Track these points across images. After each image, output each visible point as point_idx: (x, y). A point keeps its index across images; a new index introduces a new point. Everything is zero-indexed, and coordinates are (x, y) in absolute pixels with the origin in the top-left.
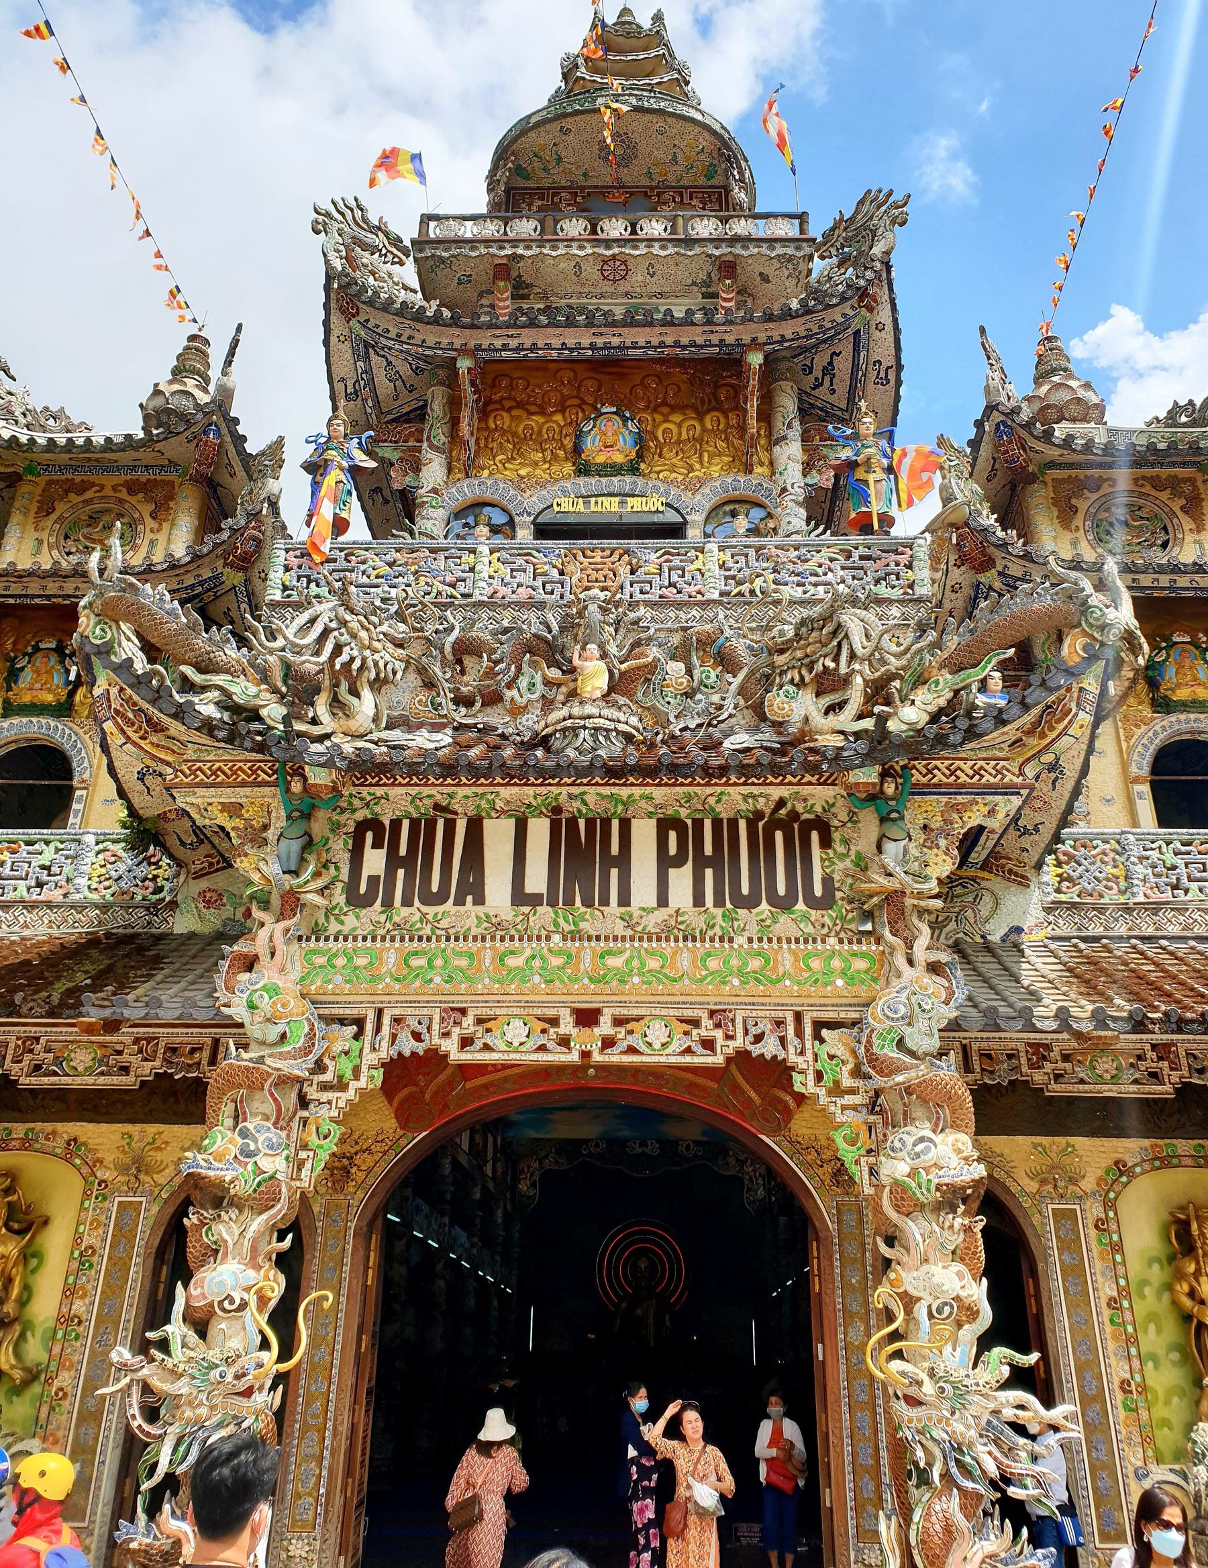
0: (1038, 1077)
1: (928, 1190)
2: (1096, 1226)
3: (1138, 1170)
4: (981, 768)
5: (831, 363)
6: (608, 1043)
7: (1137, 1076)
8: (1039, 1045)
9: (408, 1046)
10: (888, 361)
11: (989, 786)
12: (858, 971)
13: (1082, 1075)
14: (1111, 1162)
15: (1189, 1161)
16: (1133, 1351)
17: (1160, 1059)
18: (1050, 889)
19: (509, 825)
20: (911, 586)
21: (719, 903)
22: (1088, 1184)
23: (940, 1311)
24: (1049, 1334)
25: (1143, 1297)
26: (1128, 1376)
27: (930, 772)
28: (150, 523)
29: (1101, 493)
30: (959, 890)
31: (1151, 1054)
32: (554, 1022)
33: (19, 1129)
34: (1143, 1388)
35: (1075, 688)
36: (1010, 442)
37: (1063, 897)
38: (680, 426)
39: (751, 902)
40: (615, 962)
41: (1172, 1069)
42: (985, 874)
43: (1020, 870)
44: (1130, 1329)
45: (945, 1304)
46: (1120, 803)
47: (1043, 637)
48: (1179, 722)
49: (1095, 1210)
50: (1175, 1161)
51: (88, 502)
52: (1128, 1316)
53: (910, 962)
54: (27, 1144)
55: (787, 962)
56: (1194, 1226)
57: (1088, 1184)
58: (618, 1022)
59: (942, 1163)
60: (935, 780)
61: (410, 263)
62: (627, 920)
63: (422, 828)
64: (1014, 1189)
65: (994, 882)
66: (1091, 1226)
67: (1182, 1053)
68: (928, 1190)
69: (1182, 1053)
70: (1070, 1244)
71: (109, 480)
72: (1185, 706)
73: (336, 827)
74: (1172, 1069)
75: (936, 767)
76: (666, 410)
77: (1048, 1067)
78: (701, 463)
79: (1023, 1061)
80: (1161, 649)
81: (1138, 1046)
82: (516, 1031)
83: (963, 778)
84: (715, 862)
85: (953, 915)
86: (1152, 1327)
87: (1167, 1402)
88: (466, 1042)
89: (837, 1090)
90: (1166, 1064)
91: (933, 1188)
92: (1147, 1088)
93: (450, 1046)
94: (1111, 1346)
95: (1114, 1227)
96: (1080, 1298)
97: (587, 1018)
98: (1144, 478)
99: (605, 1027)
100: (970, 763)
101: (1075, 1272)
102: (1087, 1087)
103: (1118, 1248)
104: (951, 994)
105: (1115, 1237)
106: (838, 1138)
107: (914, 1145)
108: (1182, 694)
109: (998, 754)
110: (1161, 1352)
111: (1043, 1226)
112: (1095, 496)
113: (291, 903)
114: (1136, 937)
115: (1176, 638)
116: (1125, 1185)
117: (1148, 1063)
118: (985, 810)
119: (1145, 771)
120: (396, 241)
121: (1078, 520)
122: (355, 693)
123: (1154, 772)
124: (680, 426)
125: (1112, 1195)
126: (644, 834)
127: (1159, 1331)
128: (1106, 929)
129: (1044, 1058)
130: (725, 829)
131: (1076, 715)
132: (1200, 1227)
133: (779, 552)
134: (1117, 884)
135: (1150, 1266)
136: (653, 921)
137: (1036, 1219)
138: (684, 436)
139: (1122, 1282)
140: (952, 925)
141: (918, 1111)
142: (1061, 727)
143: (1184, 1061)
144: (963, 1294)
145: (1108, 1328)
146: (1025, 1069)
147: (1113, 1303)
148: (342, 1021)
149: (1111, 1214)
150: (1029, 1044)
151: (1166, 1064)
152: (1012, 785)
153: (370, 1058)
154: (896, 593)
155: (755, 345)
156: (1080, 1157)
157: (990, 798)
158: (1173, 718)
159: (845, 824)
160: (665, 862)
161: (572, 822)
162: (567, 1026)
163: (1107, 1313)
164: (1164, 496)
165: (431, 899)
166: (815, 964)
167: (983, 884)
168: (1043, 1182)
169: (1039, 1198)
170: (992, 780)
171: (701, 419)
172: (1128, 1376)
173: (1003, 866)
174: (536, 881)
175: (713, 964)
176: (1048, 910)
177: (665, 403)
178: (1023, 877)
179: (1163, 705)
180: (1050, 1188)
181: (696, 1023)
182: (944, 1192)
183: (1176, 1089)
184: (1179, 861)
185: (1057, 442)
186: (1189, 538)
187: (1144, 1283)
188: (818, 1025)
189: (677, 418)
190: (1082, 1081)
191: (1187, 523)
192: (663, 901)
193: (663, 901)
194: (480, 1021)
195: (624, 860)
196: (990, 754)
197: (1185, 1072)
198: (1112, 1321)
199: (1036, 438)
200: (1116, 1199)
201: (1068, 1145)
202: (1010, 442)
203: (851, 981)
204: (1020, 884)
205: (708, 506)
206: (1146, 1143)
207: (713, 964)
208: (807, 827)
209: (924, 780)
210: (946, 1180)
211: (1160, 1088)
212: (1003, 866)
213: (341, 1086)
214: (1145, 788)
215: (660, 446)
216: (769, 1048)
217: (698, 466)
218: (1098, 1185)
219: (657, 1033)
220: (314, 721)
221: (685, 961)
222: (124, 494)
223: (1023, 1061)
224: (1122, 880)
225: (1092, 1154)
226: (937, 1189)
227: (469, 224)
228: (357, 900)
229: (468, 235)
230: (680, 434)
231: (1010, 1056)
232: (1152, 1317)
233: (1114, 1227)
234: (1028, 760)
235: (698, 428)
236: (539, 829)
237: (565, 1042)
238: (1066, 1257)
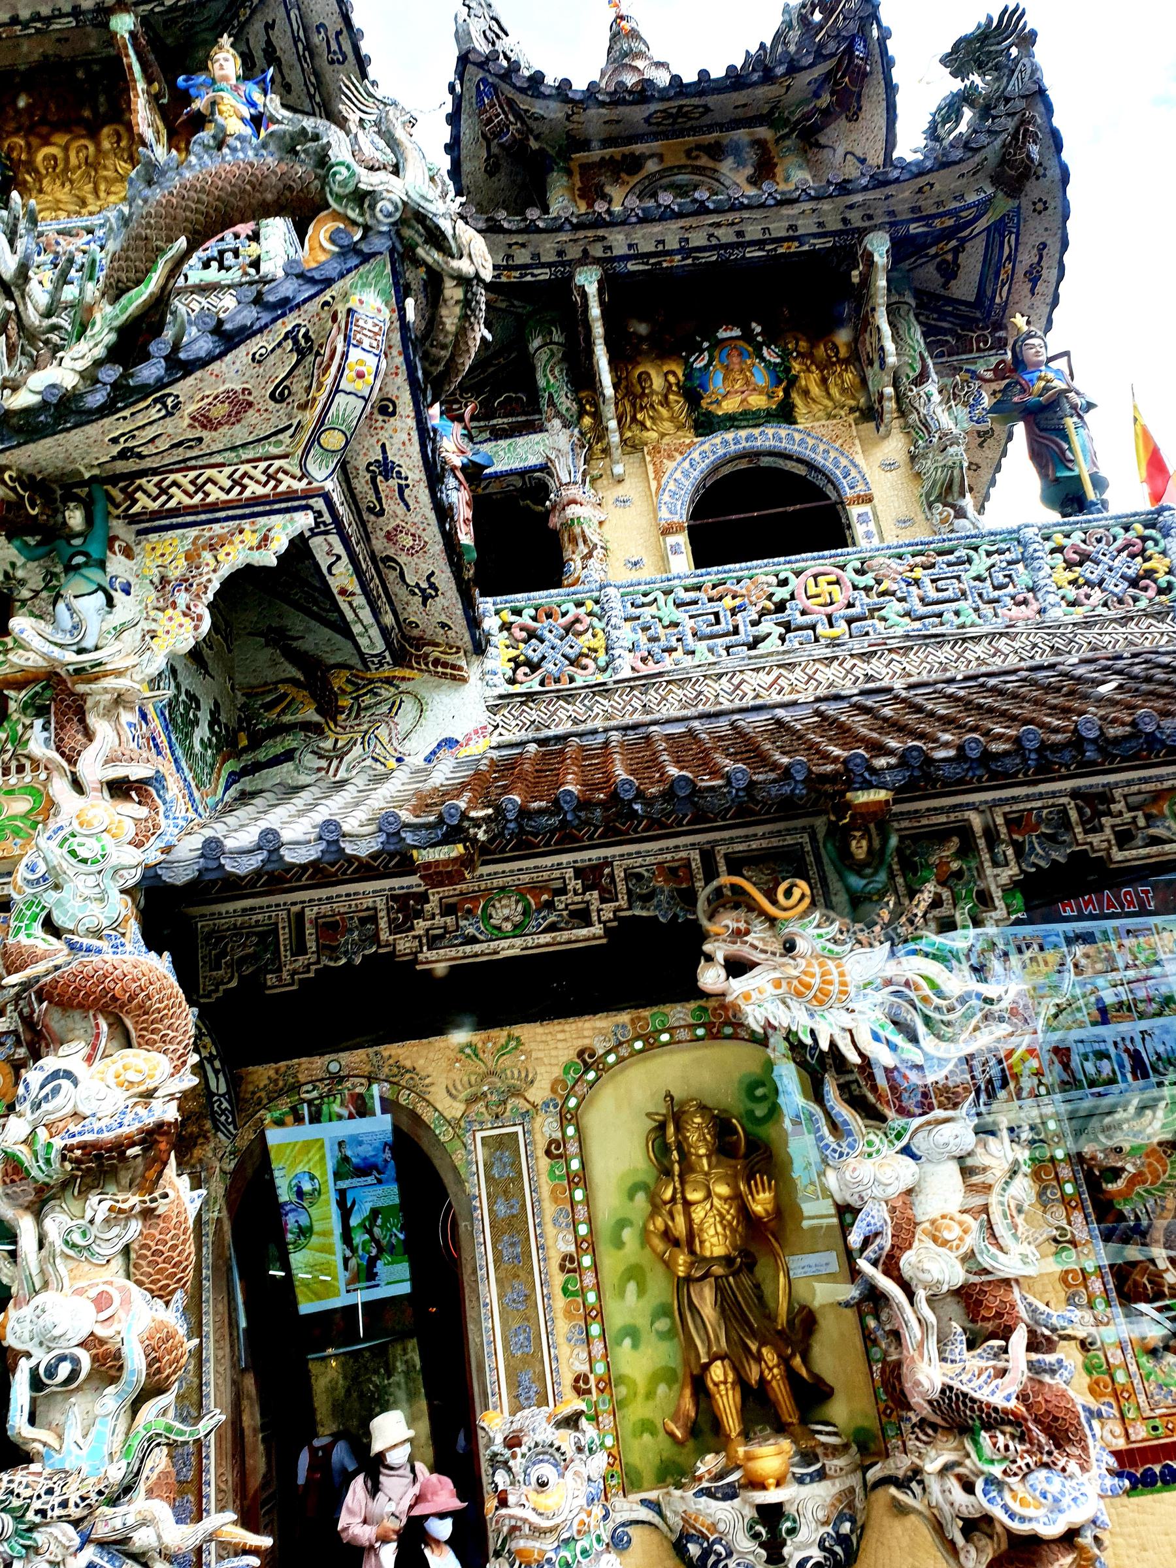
0: (404, 945)
1: (48, 1161)
2: (548, 1153)
3: (611, 1058)
4: (245, 474)
5: (269, 42)
7: (553, 918)
8: (408, 896)
10: (334, 23)
11: (256, 501)
12: (14, 817)
13: (471, 931)
14: (572, 1054)
15: (683, 1034)
16: (595, 1329)
17: (586, 889)
18: (499, 680)
23: (51, 1372)
24: (471, 1327)
25: (619, 1244)
26: (585, 1368)
27: (163, 491)
29: (643, 173)
30: (368, 700)
31: (575, 884)
34: (608, 1383)
35: (341, 316)
36: (492, 106)
37: (517, 689)
38: (66, 149)
41: (603, 900)
42: (407, 673)
43: (450, 659)
44: (591, 1297)
45: (62, 1358)
47: (545, 357)
48: (725, 443)
49: (546, 1127)
50: (665, 1037)
52: (589, 1279)
53: (77, 785)
56: (671, 1129)
57: (539, 1093)
59: (85, 1110)
60: (172, 504)
64: (428, 1116)
65: (418, 681)
66: (540, 1153)
67: (620, 874)
68: (48, 1161)
69: (620, 874)
70: (506, 1186)
72: (732, 421)
74: (603, 900)
75: (174, 483)
76: (44, 130)
77: (421, 925)
78: (96, 191)
79: (383, 924)
80: (702, 352)
81: (556, 874)
83: (215, 494)
85: (359, 736)
86: (632, 1287)
87: (650, 1395)
90: (596, 894)
91: (54, 1155)
92: (565, 936)
94: (562, 1326)
95: (573, 1148)
98: (699, 147)
100: (228, 470)
101: (511, 1228)
102: (477, 948)
103: (582, 1179)
105: (575, 1165)
107: (42, 1087)
108: (730, 406)
109: (275, 451)
110: (642, 1322)
111: (470, 1163)
112: (637, 178)
114: (616, 729)
115: (722, 334)
116: (592, 1084)
117: (570, 898)
118: (254, 540)
123: (695, 515)
124: (66, 149)
125: (572, 1102)
127: (641, 1291)
128: (576, 722)
129: (419, 914)
131: (345, 355)
132: (678, 1129)
133: (61, 239)
134: (595, 660)
135: (631, 1197)
137: (458, 1157)
138: (73, 161)
139: (583, 1230)
140: (357, 750)
142: (328, 380)
143: (621, 887)
144: (101, 1332)
145: (560, 1302)
146: (384, 936)
149: (571, 1131)
150: (394, 898)
151: (596, 894)
152: (290, 495)
156: (528, 1054)
157: (262, 521)
158: (717, 439)
159: (37, 593)
163: (558, 1279)
167: (403, 686)
168: (472, 1100)
170: (260, 491)
171: (94, 135)
172: (585, 1368)
173: (426, 656)
176: (493, 709)
177: (44, 121)
178: (454, 667)
179: (705, 425)
180: (480, 1106)
182: (77, 1161)
183: (607, 930)
184: (680, 615)
185: (547, 92)
187: (622, 1223)
189: (61, 139)
190: (473, 940)
196: (260, 451)
197: (623, 903)
198: (565, 1291)
199: (522, 90)
200: (578, 1106)
201: (510, 1037)
202: (492, 106)
204: (454, 678)
206: (624, 1017)
209: (155, 506)
210: (89, 1137)
211: (584, 932)
212: (426, 656)
214: (682, 539)
215: (39, 179)
217: (90, 198)
218: (553, 1090)
223: (383, 924)
224: (602, 652)
225: (548, 1048)
226: (64, 1158)
230: (67, 159)
231: (363, 921)
232: (634, 1273)
233: (573, 1148)
234: (307, 451)
235: (92, 149)
238: (501, 1209)
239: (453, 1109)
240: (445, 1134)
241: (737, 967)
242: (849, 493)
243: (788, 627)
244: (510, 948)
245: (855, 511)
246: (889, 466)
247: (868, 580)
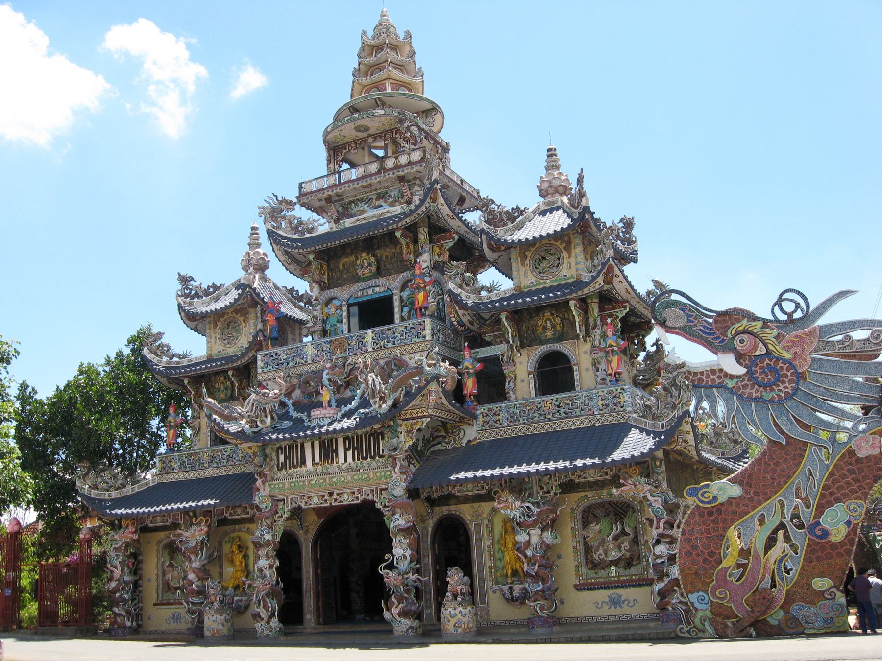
0: (453, 492)
6: (336, 500)
9: (294, 505)
19: (310, 443)
20: (425, 337)
21: (358, 460)
22: (485, 515)
28: (244, 324)
32: (324, 496)
33: (237, 527)
39: (365, 459)
40: (334, 480)
46: (526, 382)
49: (486, 522)
51: (226, 320)
54: (240, 530)
55: (371, 475)
57: (485, 515)
58: (338, 494)
61: (297, 206)
62: (338, 467)
63: (291, 447)
70: (478, 532)
71: (230, 311)
73: (273, 449)
82: (316, 500)
84: (357, 448)
88: (306, 503)
89: (385, 507)
93: (302, 505)
96: (479, 547)
97: (331, 494)
99: (335, 497)
101: (479, 539)
103: (492, 532)
104: (405, 480)
106: (385, 518)
113: (261, 474)
119: (532, 370)
120: (290, 203)
121: (527, 262)
122: (266, 416)
126: (341, 441)
130: (359, 438)
136: (344, 467)
141: (398, 510)
147: (489, 547)
148: (281, 501)
153: (287, 509)
154: (421, 340)
155: (398, 229)
160: (346, 450)
161: (324, 441)
162: (326, 497)
164: (558, 243)
165: (295, 467)
166: (378, 474)
169: (471, 521)
174: (317, 460)
175: (356, 477)
181: (354, 493)
186: (566, 262)
188: (382, 490)
191: (566, 254)
192: (346, 461)
193: (346, 461)
194: (309, 497)
195: (336, 452)
203: (386, 478)
205: (399, 286)
207: (356, 477)
208: (379, 434)
213: (282, 517)
216: (370, 497)
219: (346, 496)
220: (257, 426)
221: (349, 478)
222: (234, 315)
227: (314, 182)
228: (280, 469)
229: (315, 189)
236: (317, 444)
237: (326, 501)
239: (469, 517)
240: (468, 522)
241: (499, 504)
242: (573, 363)
243: (540, 414)
244: (470, 493)
245: (575, 368)
246: (586, 353)
247: (557, 403)
